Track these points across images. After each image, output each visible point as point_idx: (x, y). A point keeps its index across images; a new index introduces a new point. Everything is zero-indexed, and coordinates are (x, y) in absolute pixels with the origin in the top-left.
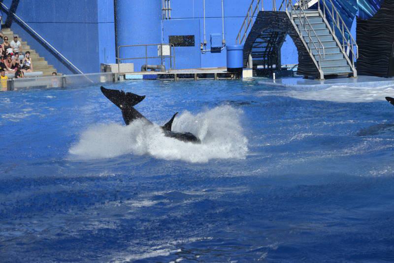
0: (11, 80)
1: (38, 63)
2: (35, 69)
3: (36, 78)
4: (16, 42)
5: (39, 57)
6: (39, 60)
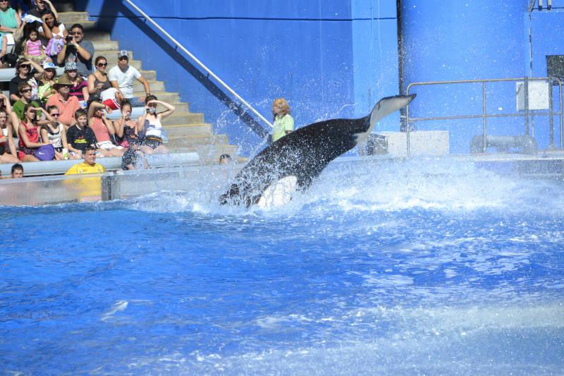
0: (112, 174)
1: (182, 129)
2: (175, 144)
3: (180, 170)
4: (124, 69)
5: (188, 114)
6: (189, 120)
